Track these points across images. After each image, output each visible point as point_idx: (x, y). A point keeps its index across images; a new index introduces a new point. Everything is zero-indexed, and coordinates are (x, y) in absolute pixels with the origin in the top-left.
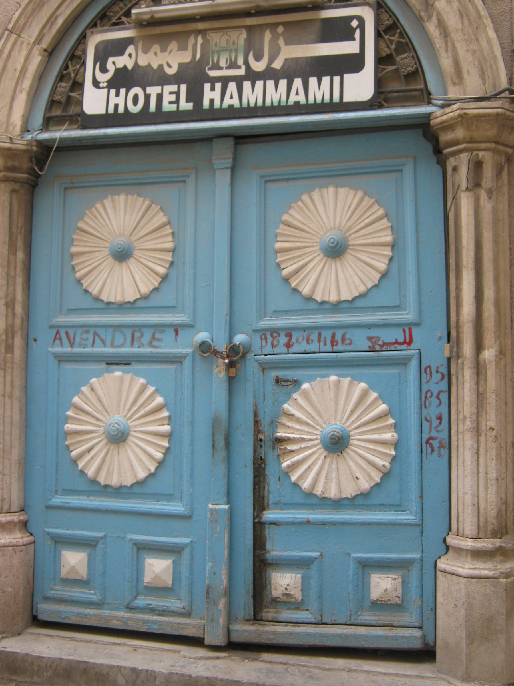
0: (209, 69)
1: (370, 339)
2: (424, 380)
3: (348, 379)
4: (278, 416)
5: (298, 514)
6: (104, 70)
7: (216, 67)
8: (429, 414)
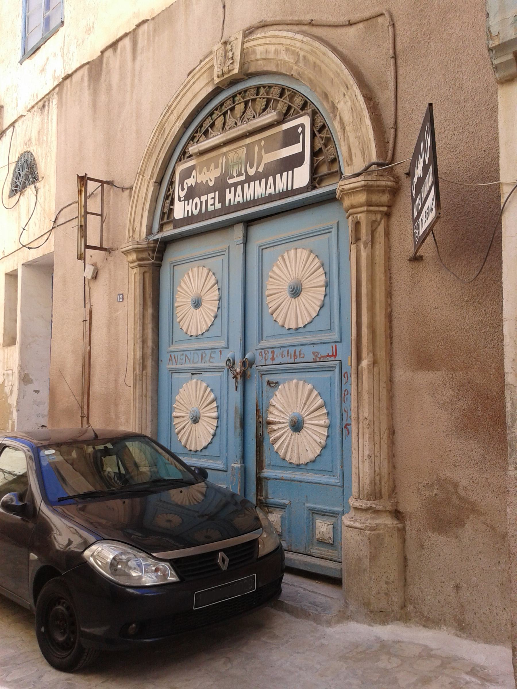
0: (229, 179)
1: (314, 353)
2: (343, 382)
3: (302, 382)
4: (269, 407)
5: (279, 473)
7: (232, 177)
8: (346, 407)
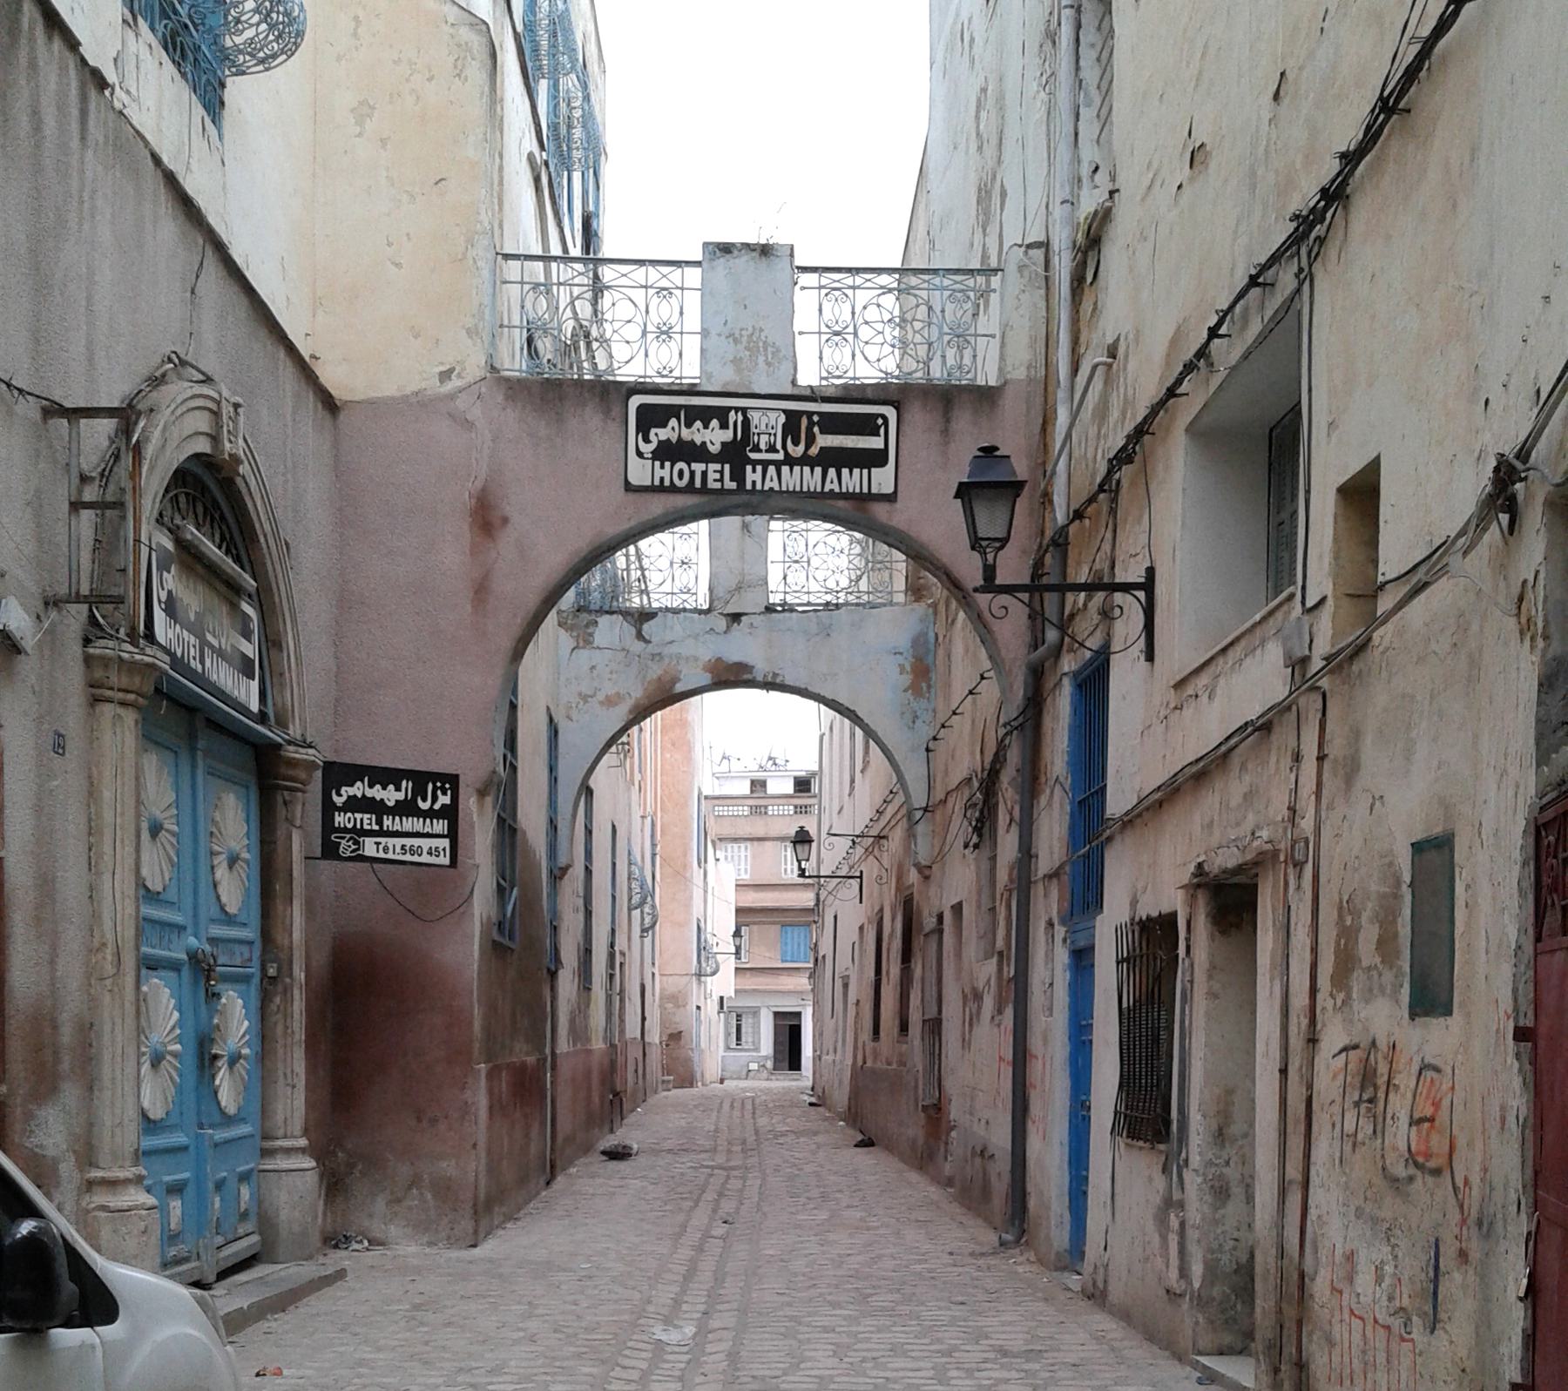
6: (647, 440)
7: (757, 449)
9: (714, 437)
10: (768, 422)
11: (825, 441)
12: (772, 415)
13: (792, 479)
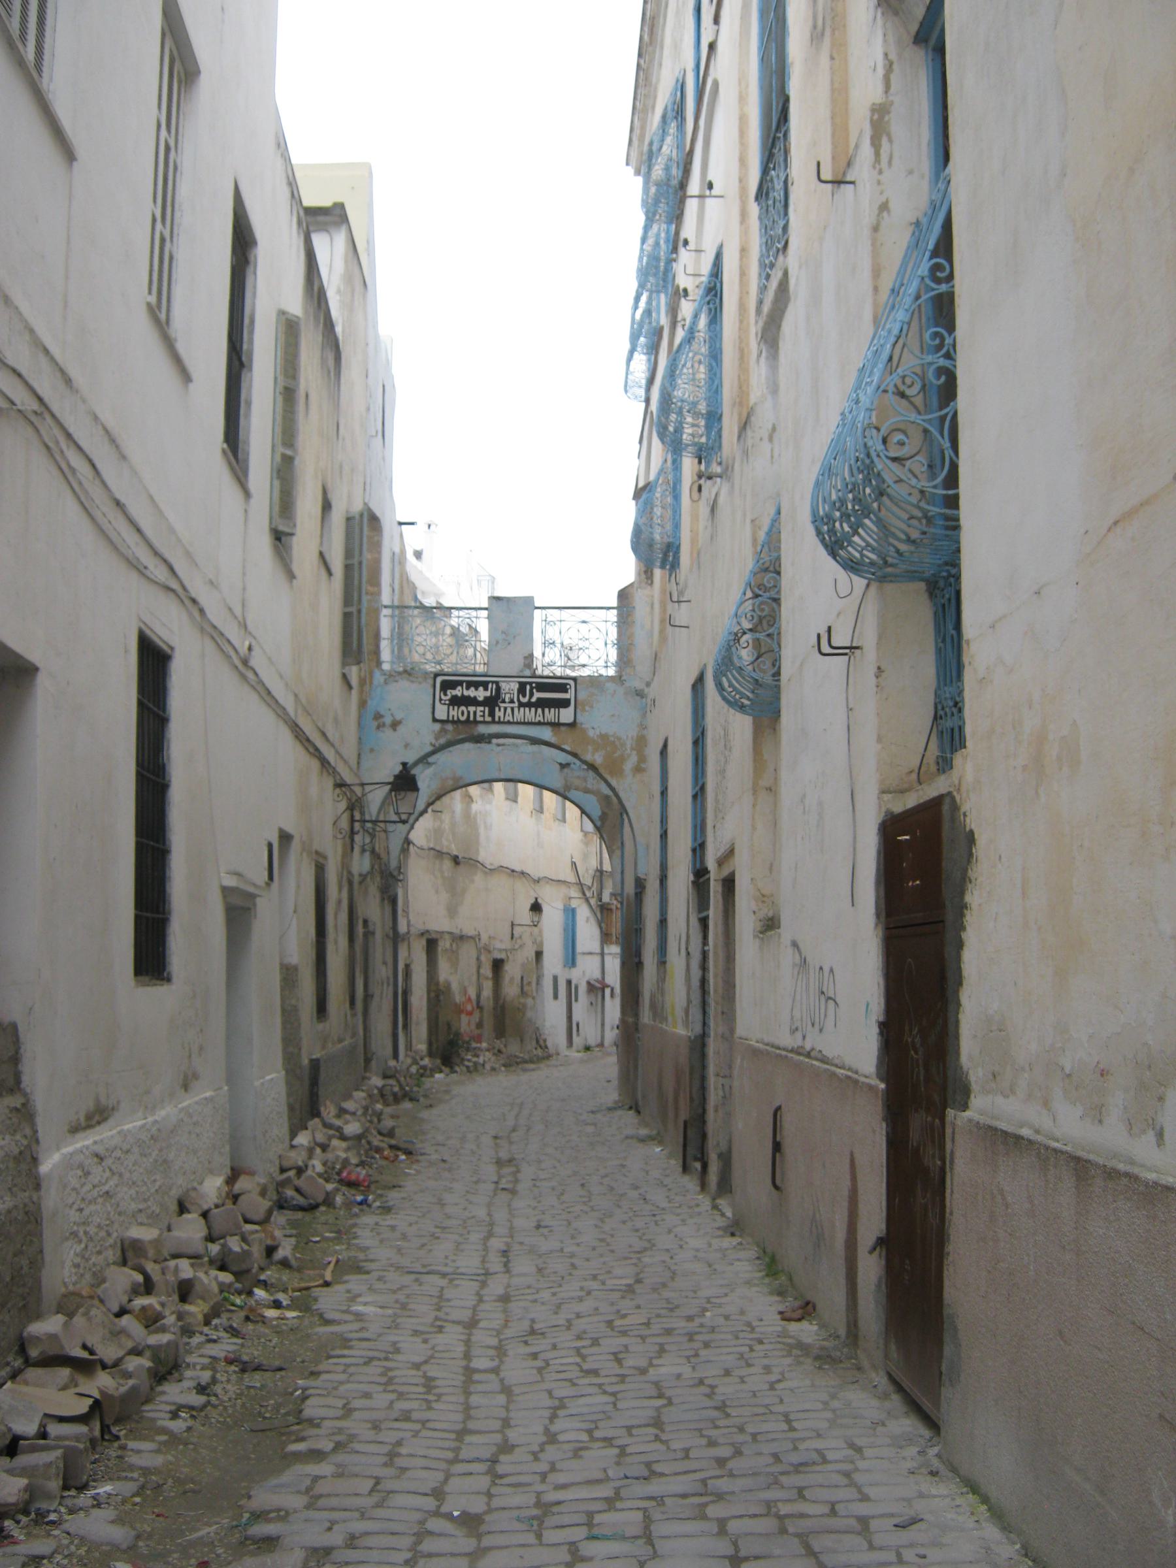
6: (445, 695)
9: (481, 694)
10: (510, 688)
11: (537, 695)
12: (512, 684)
13: (519, 715)
